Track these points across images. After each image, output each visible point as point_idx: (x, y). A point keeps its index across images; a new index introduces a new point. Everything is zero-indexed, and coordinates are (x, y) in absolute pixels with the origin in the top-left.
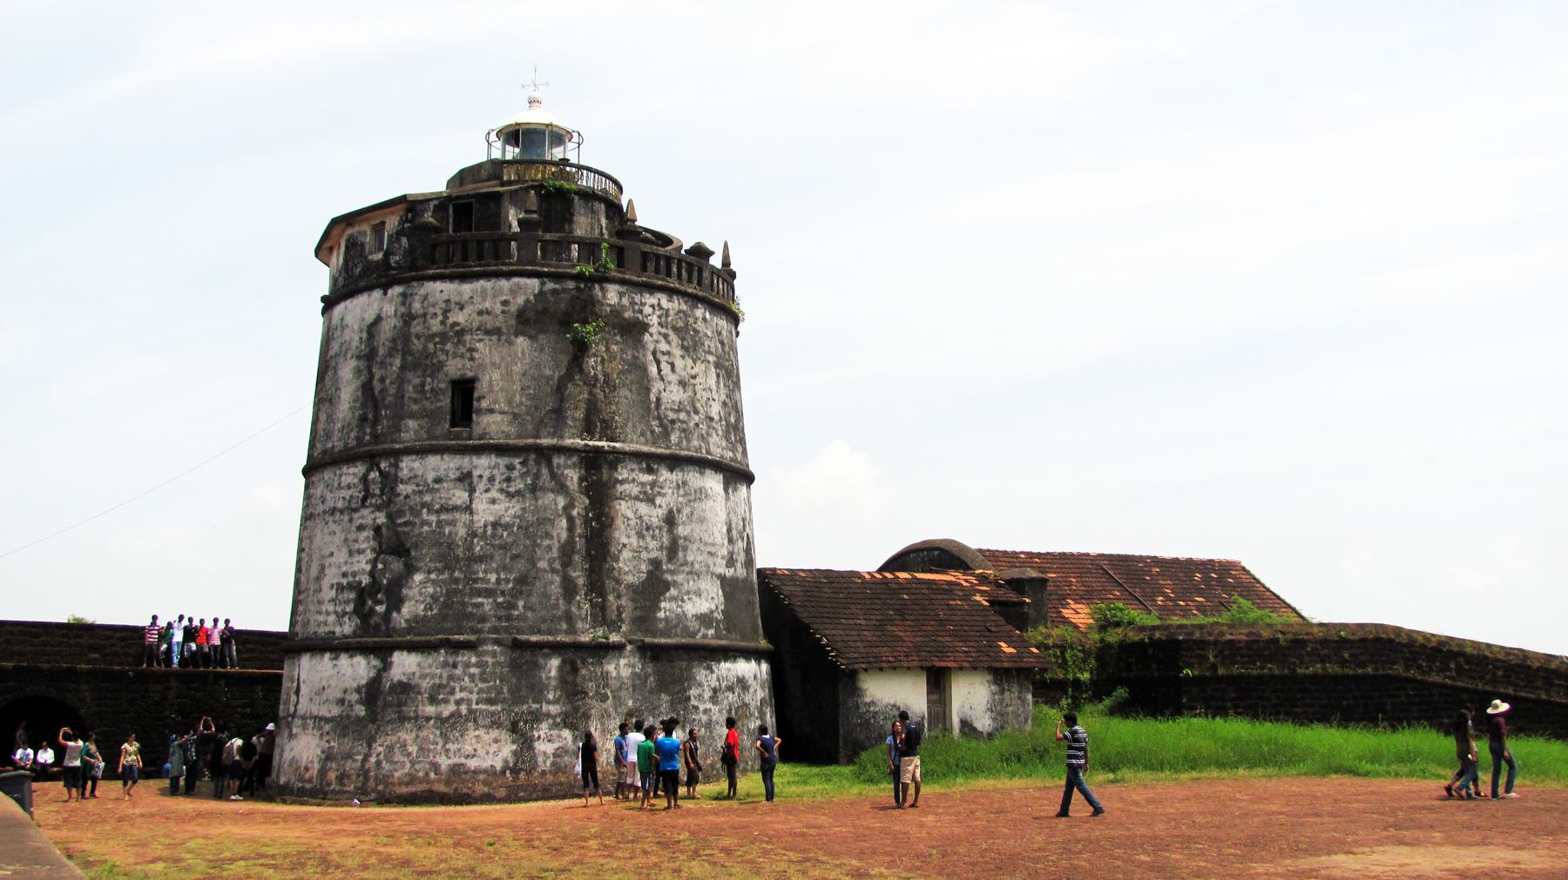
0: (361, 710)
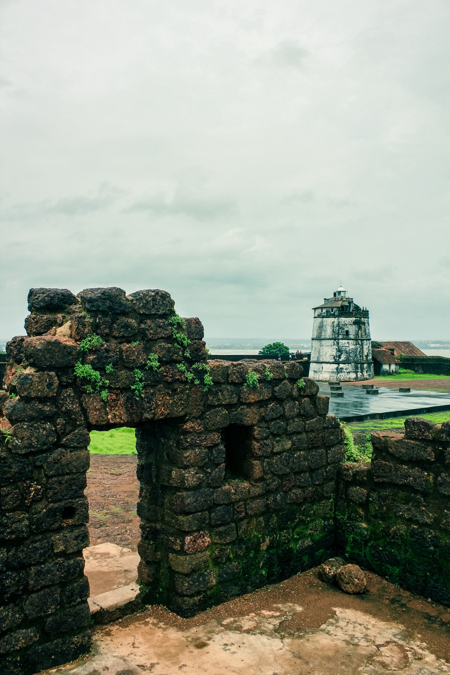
0: (336, 371)
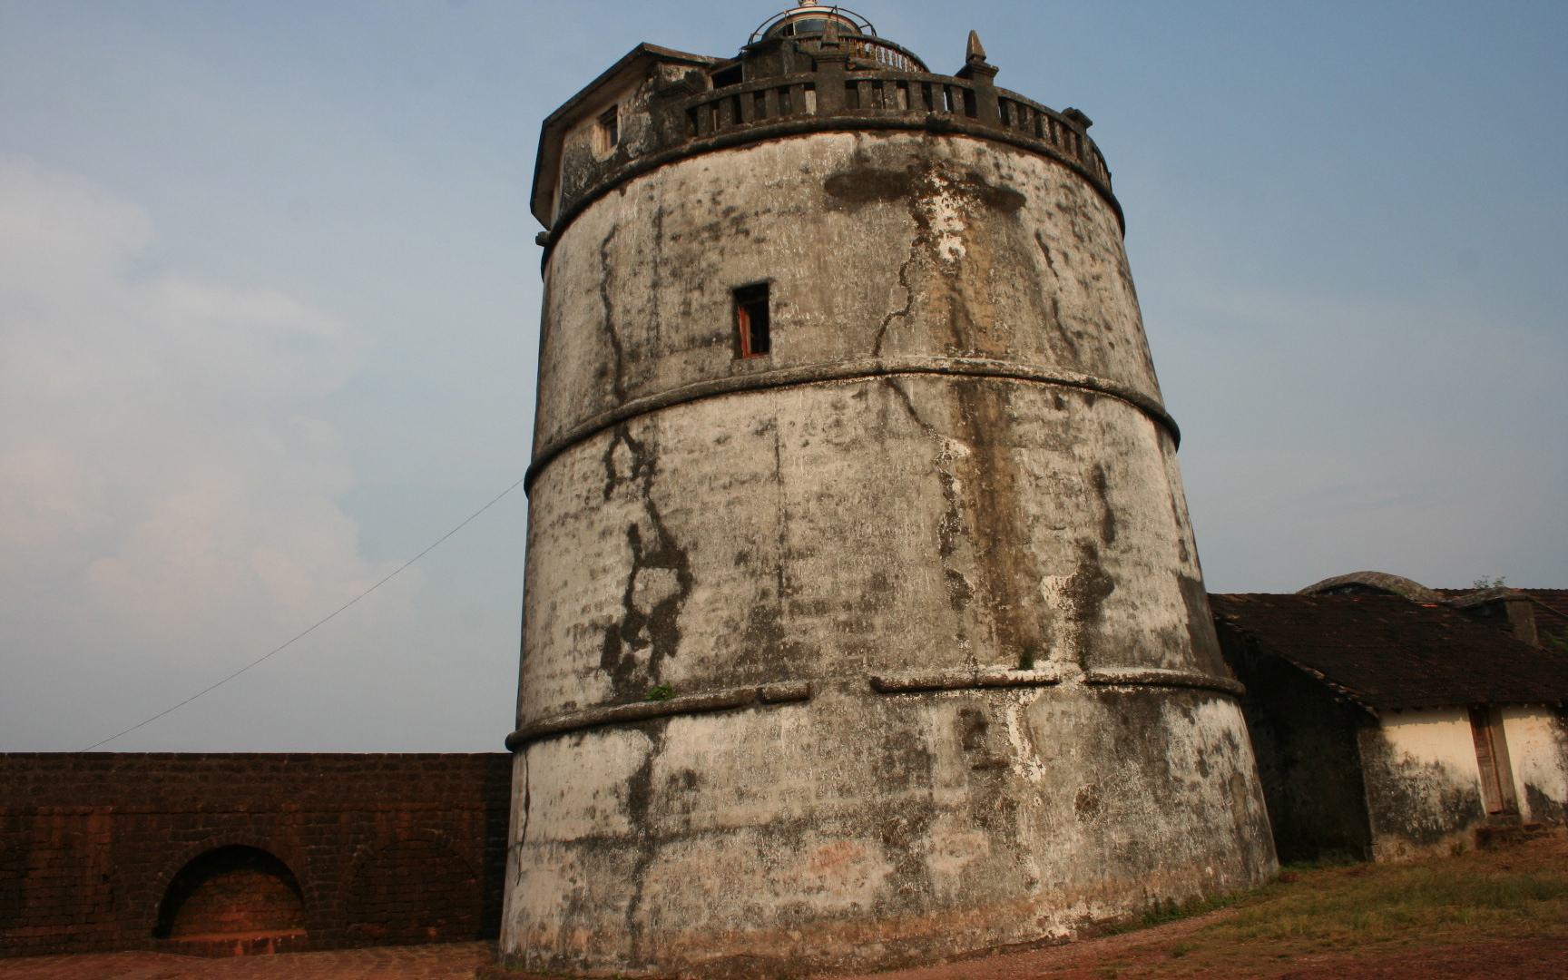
0: (622, 825)
